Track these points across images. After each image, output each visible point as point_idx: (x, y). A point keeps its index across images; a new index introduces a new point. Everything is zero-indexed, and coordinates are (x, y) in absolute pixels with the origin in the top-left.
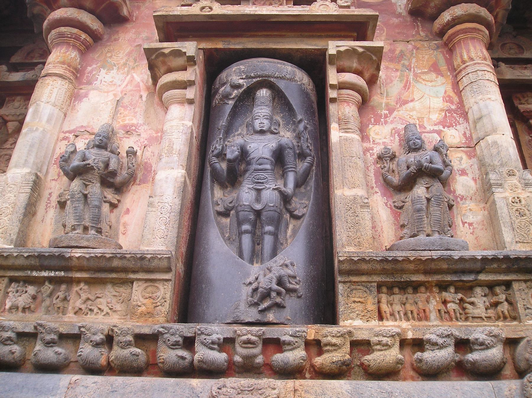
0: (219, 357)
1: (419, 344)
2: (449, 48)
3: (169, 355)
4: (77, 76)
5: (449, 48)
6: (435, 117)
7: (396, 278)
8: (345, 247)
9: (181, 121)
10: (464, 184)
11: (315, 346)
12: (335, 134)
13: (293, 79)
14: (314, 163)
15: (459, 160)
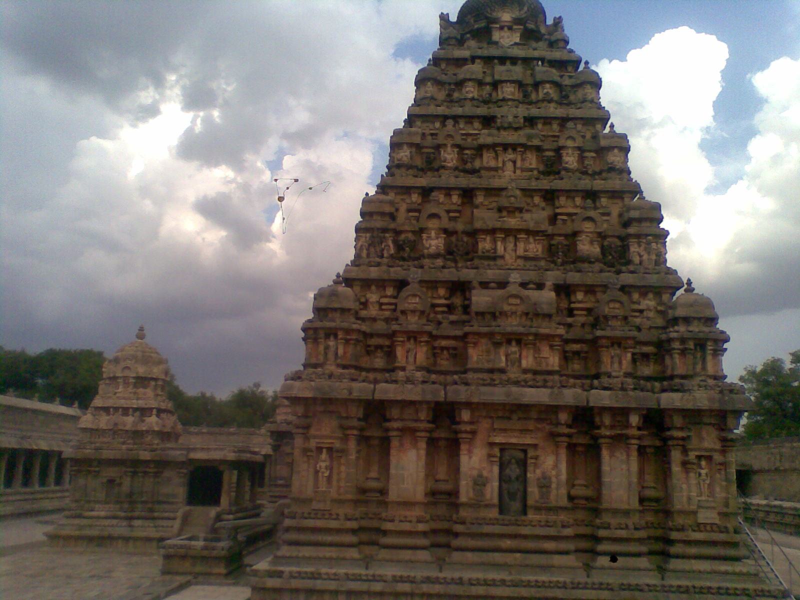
0: (508, 523)
1: (540, 521)
2: (557, 447)
3: (501, 522)
4: (470, 452)
5: (557, 447)
6: (551, 467)
7: (538, 509)
8: (530, 502)
9: (496, 469)
10: (554, 486)
11: (524, 521)
12: (529, 475)
13: (521, 455)
14: (524, 480)
15: (554, 480)
